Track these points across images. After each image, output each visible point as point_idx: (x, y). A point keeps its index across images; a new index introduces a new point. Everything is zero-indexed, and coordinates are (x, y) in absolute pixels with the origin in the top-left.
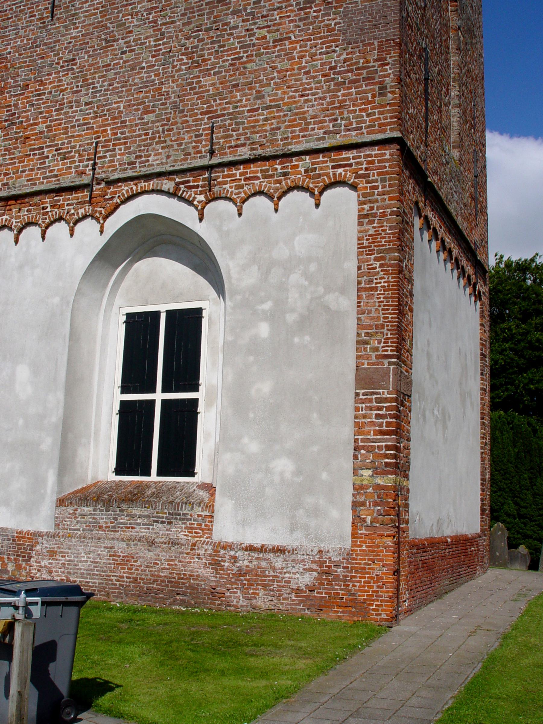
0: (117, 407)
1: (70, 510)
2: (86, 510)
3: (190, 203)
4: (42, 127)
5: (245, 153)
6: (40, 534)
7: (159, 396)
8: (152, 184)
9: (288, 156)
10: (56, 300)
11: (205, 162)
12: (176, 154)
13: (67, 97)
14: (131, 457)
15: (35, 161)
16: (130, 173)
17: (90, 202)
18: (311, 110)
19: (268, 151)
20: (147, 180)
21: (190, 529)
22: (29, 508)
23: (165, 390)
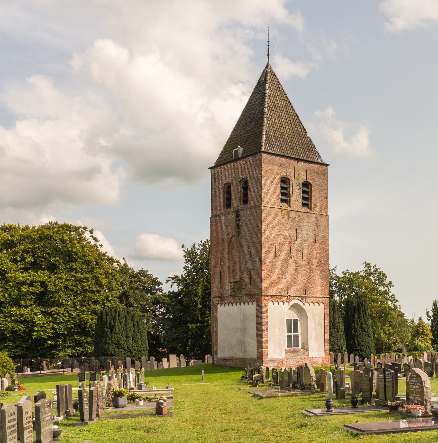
4: (276, 281)
5: (310, 295)
6: (283, 359)
7: (293, 334)
9: (316, 297)
11: (305, 296)
13: (281, 276)
14: (289, 345)
15: (275, 288)
16: (294, 295)
19: (314, 296)
22: (281, 354)
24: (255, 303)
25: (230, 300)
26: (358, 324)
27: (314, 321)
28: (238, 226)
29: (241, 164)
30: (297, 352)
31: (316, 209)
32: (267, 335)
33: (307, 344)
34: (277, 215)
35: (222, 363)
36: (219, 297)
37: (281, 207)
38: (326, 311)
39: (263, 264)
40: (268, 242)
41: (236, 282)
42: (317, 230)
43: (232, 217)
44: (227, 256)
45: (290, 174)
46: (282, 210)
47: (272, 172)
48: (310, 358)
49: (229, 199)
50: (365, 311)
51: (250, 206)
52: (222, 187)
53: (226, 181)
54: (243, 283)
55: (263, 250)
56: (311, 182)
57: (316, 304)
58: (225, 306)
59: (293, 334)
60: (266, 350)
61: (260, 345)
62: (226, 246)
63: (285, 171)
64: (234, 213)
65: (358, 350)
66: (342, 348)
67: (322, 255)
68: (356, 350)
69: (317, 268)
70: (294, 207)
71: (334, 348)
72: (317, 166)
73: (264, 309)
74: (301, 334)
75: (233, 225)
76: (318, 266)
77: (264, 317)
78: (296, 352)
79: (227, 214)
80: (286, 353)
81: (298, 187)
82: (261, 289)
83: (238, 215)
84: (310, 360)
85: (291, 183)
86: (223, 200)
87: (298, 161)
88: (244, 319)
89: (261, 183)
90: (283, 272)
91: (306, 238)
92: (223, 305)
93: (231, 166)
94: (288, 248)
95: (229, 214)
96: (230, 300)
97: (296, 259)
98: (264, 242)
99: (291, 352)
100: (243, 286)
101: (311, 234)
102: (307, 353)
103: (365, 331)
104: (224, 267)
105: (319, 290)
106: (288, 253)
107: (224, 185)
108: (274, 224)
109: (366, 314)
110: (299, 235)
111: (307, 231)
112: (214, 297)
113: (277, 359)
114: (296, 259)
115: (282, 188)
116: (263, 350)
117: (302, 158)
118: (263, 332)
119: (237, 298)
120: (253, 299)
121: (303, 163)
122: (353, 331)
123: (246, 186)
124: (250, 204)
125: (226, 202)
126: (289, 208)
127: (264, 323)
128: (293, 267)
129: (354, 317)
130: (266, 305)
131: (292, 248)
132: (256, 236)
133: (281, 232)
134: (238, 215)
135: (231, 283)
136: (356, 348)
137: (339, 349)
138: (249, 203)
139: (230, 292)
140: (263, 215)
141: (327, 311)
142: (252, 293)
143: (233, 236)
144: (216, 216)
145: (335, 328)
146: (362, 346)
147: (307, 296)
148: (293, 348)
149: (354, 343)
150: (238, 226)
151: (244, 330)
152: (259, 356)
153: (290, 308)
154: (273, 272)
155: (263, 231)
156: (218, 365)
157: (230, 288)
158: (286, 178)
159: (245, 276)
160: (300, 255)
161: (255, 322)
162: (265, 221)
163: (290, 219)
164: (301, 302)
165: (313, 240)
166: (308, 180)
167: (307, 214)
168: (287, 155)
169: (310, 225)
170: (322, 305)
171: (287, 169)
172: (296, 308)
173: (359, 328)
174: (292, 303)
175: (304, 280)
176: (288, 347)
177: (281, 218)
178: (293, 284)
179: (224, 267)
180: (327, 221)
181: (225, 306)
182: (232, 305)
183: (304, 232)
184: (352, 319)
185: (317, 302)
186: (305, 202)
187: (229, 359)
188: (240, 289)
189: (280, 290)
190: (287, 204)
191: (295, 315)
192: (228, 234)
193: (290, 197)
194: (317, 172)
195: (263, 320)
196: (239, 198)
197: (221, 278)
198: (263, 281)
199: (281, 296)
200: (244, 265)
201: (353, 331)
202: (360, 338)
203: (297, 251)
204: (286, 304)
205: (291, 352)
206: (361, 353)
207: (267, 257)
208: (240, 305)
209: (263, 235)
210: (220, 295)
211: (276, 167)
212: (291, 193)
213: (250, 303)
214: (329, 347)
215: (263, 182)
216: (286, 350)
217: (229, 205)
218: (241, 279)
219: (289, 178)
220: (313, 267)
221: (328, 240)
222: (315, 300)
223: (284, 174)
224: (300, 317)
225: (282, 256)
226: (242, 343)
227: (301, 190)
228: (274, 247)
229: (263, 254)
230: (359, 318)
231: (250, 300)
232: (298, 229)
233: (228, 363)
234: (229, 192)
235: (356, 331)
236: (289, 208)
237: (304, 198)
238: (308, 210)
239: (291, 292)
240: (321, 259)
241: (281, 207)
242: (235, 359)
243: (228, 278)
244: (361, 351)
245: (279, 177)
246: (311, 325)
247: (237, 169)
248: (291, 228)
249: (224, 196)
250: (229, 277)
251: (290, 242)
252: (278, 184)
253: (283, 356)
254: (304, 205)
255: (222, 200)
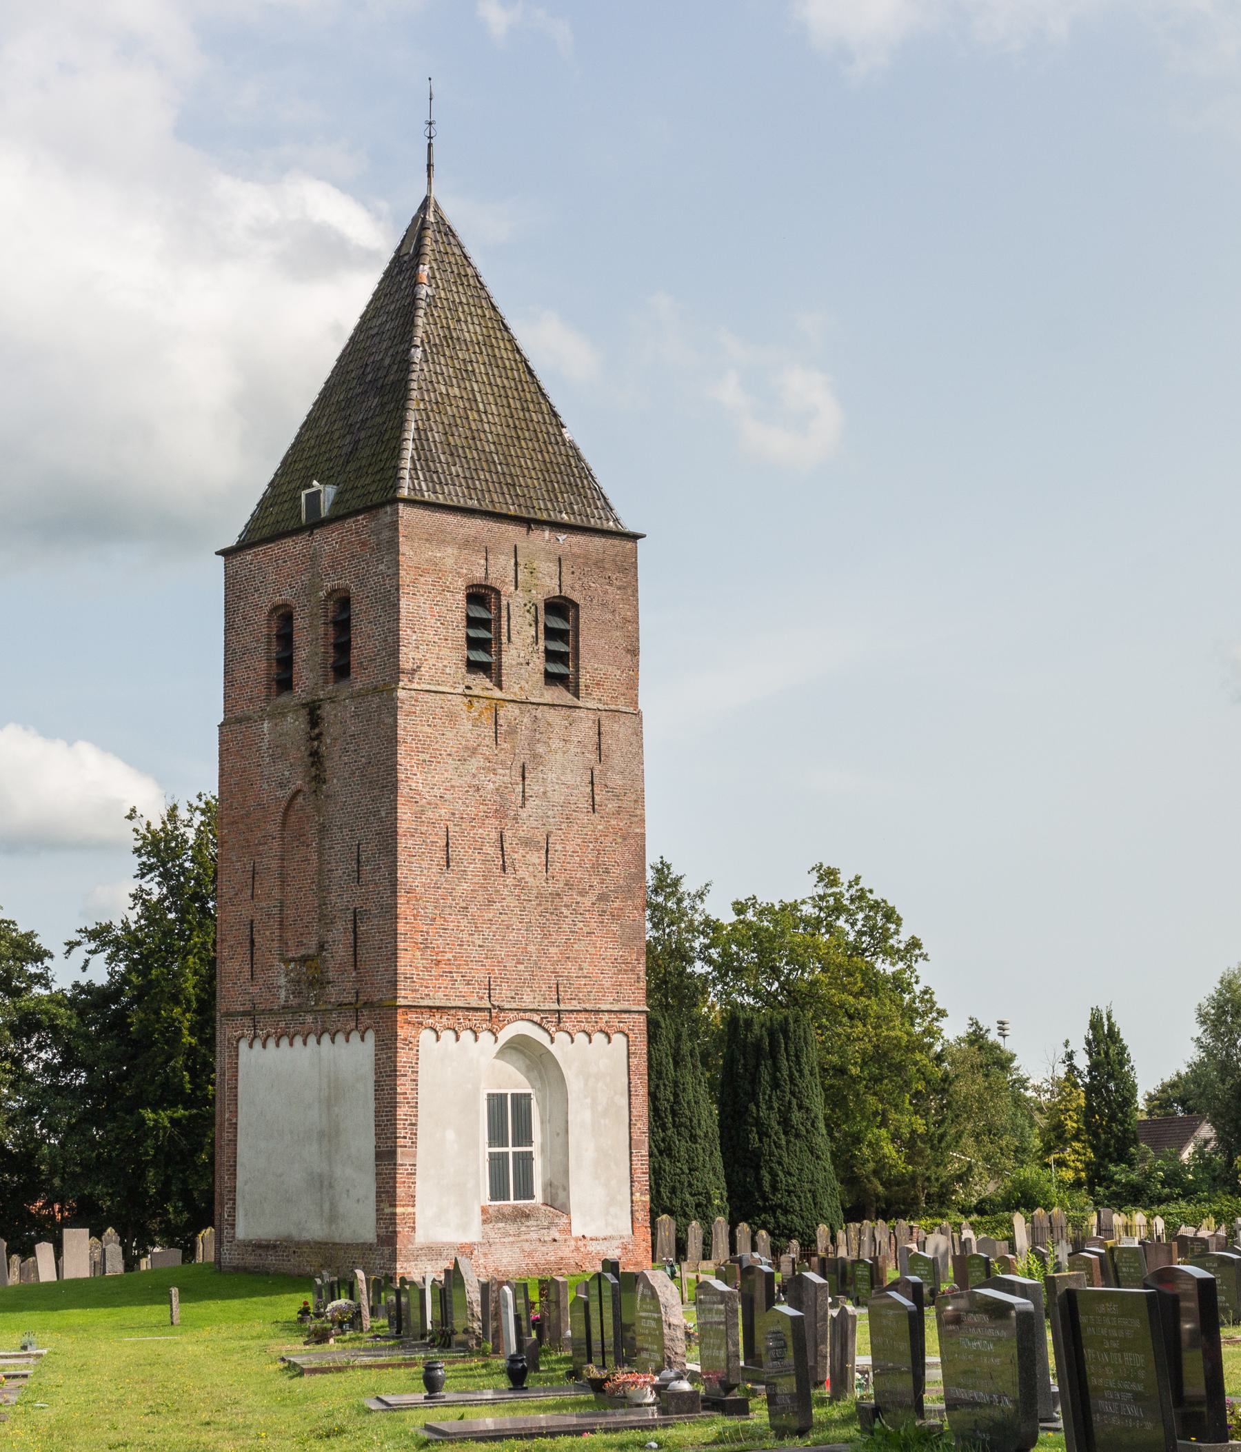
0: (487, 1157)
1: (491, 1226)
2: (501, 1225)
3: (547, 1031)
4: (449, 956)
5: (574, 1005)
7: (510, 1149)
8: (528, 1015)
9: (598, 1011)
10: (470, 1086)
11: (555, 1006)
12: (539, 998)
13: (465, 936)
14: (498, 1191)
15: (445, 982)
16: (514, 1006)
17: (490, 1021)
18: (607, 984)
19: (588, 1006)
20: (523, 1012)
21: (559, 1231)
23: (514, 1146)
24: (370, 1036)
25: (282, 1025)
26: (770, 1108)
27: (588, 1100)
28: (316, 757)
29: (328, 541)
30: (528, 1216)
31: (596, 693)
32: (415, 1156)
33: (566, 1188)
34: (452, 717)
35: (250, 1260)
36: (244, 1014)
37: (468, 688)
38: (634, 1061)
39: (401, 893)
40: (418, 815)
41: (304, 960)
42: (598, 768)
43: (295, 724)
44: (274, 864)
45: (500, 571)
46: (471, 698)
47: (435, 567)
48: (577, 1239)
49: (285, 662)
50: (797, 1057)
51: (358, 686)
52: (262, 617)
53: (278, 599)
54: (331, 965)
55: (403, 843)
56: (576, 596)
57: (599, 1038)
58: (264, 1046)
59: (510, 1149)
60: (410, 1210)
61: (386, 1192)
62: (273, 828)
63: (483, 562)
64: (304, 712)
65: (772, 1210)
66: (709, 1199)
67: (618, 858)
68: (765, 1210)
69: (602, 905)
70: (516, 688)
71: (677, 1202)
72: (598, 542)
73: (403, 1057)
74: (543, 1151)
75: (298, 753)
76: (602, 898)
77: (403, 1086)
78: (522, 1216)
79: (277, 715)
80: (484, 1222)
81: (530, 617)
82: (394, 984)
83: (314, 720)
84: (577, 1249)
85: (504, 602)
86: (264, 665)
87: (529, 528)
88: (333, 1095)
89: (396, 606)
90: (473, 922)
91: (557, 798)
92: (258, 1044)
93: (294, 546)
94: (494, 835)
95: (284, 715)
96: (282, 1025)
97: (520, 874)
98: (405, 814)
99: (502, 1217)
100: (331, 975)
101: (578, 780)
102: (564, 1220)
103: (797, 1136)
104: (263, 904)
105: (607, 984)
106: (492, 851)
107: (271, 612)
108: (445, 749)
109: (800, 1071)
110: (533, 788)
111: (564, 773)
112: (229, 1014)
113: (450, 1246)
114: (520, 874)
115: (472, 622)
116: (399, 1210)
117: (545, 516)
118: (400, 1142)
119: (309, 1018)
120: (365, 1021)
121: (547, 534)
122: (754, 1136)
123: (345, 616)
124: (359, 680)
125: (274, 670)
126: (497, 694)
127: (402, 1112)
128: (511, 902)
129: (755, 1080)
130: (411, 1044)
131: (508, 834)
132: (376, 792)
133: (468, 779)
134: (314, 720)
135: (287, 961)
136: (766, 1199)
137: (698, 1205)
138: (353, 675)
139: (283, 994)
140: (401, 721)
141: (640, 1062)
142: (363, 998)
143: (299, 791)
144: (239, 721)
145: (682, 1125)
146: (789, 1192)
147: (562, 1007)
148: (512, 1202)
149: (759, 1180)
150: (316, 757)
151: (330, 1136)
152: (383, 1232)
153: (501, 1054)
154: (439, 921)
155: (401, 776)
156: (236, 1269)
157: (282, 981)
158: (486, 587)
159: (339, 936)
160: (537, 858)
161: (372, 1105)
162: (409, 739)
163: (502, 730)
164: (541, 1032)
165: (585, 804)
166: (567, 592)
167: (564, 711)
168: (490, 508)
169: (573, 749)
170: (619, 1039)
171: (490, 557)
172: (524, 1054)
173: (774, 1124)
174: (506, 1034)
175: (553, 950)
176: (493, 1198)
177: (468, 728)
178: (510, 964)
179: (263, 904)
180: (638, 733)
181: (264, 1046)
182: (291, 1044)
183: (551, 776)
184: (749, 1088)
185: (601, 1031)
186: (556, 668)
187: (275, 1247)
188: (319, 982)
189: (464, 989)
190: (490, 677)
191: (521, 1078)
192: (282, 786)
193: (499, 652)
194: (599, 564)
195: (400, 1098)
196: (318, 659)
197: (252, 942)
198: (401, 954)
199: (468, 1009)
200: (333, 897)
201: (754, 1136)
202: (780, 1163)
203: (527, 843)
204: (485, 1036)
205: (502, 1217)
206: (782, 1219)
207: (416, 869)
208: (319, 1042)
209: (403, 790)
210: (248, 1007)
211: (450, 550)
212: (504, 639)
213: (355, 1036)
214: (647, 1198)
215: (403, 603)
216: (484, 1210)
217: (284, 683)
218: (321, 947)
219: (497, 585)
220: (587, 902)
221: (639, 800)
222: (594, 1020)
223: (479, 574)
224: (538, 1085)
225: (472, 864)
226: (322, 1184)
227: (541, 627)
228: (442, 833)
229: (402, 856)
230: (776, 1085)
231: (353, 1024)
232: (529, 766)
233: (271, 1260)
234: (285, 638)
235: (763, 1134)
236: (497, 694)
237: (551, 656)
238: (568, 698)
239: (502, 995)
240: (615, 871)
241: (468, 688)
242: (299, 1244)
243: (276, 944)
244: (786, 1212)
245: (461, 584)
246: (580, 1115)
247: (314, 558)
248: (503, 763)
249: (269, 651)
250: (281, 939)
251: (500, 813)
252: (456, 607)
253: (474, 1233)
254: (551, 679)
255: (260, 665)
